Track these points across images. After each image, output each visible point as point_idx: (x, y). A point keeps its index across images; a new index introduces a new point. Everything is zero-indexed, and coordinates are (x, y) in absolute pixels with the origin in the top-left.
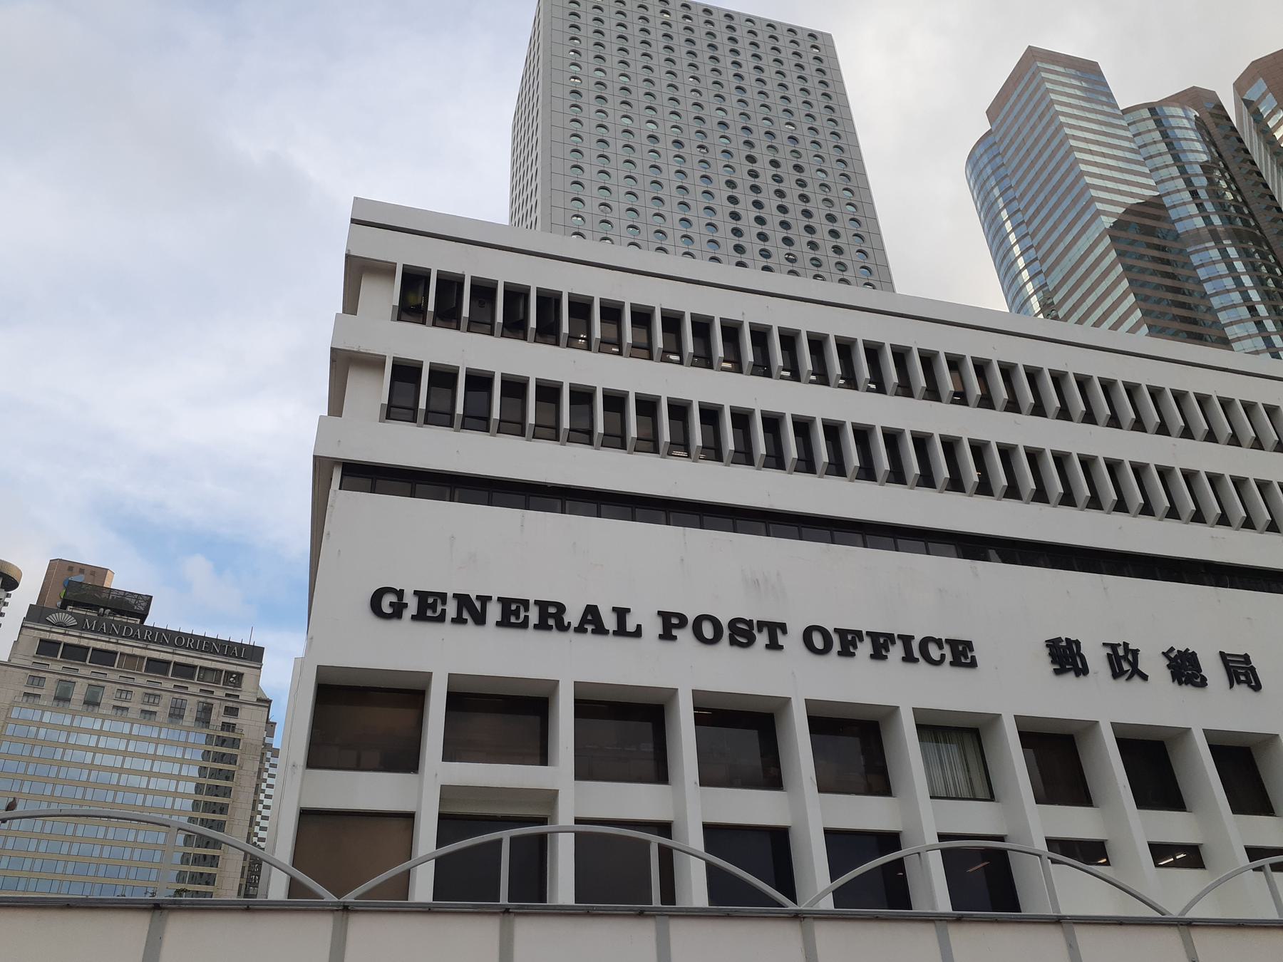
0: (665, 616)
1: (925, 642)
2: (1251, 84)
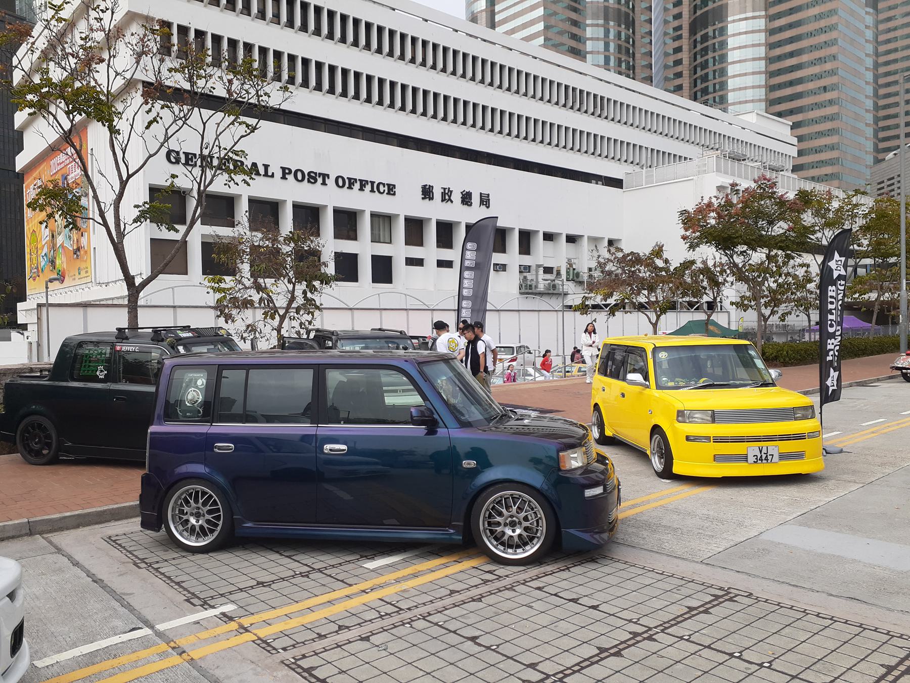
0: (283, 169)
1: (379, 184)
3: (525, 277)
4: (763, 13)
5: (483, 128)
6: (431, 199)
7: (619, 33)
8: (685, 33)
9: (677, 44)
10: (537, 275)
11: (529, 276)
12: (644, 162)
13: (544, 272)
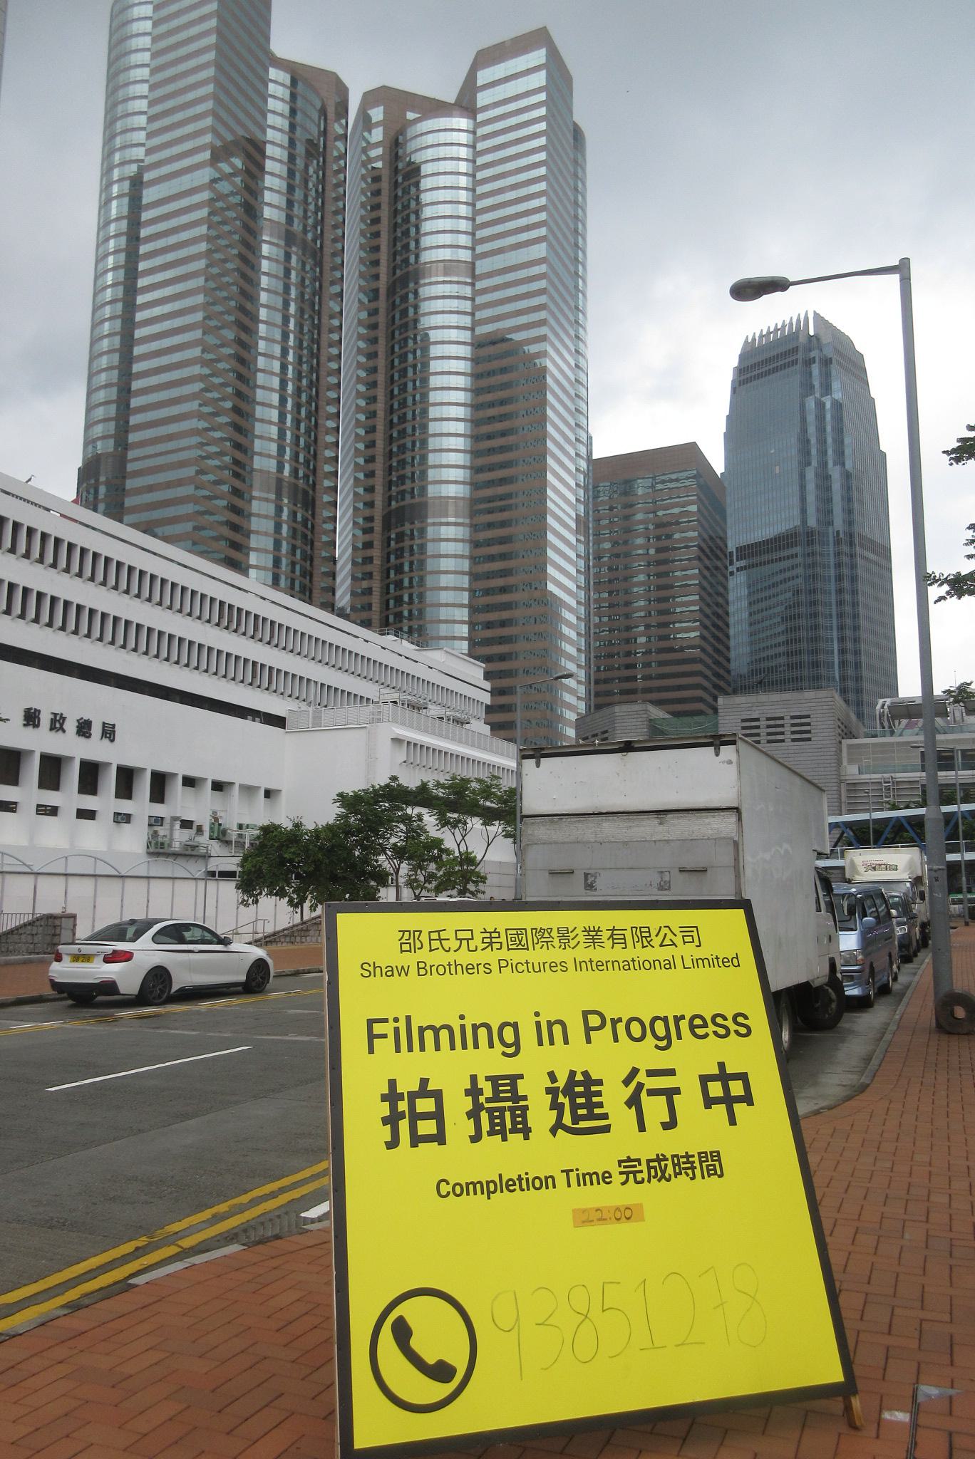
2: (375, 104)
3: (156, 832)
4: (467, 521)
5: (112, 643)
6: (36, 726)
7: (295, 514)
8: (378, 525)
9: (368, 538)
10: (172, 830)
11: (162, 831)
12: (312, 698)
13: (182, 827)
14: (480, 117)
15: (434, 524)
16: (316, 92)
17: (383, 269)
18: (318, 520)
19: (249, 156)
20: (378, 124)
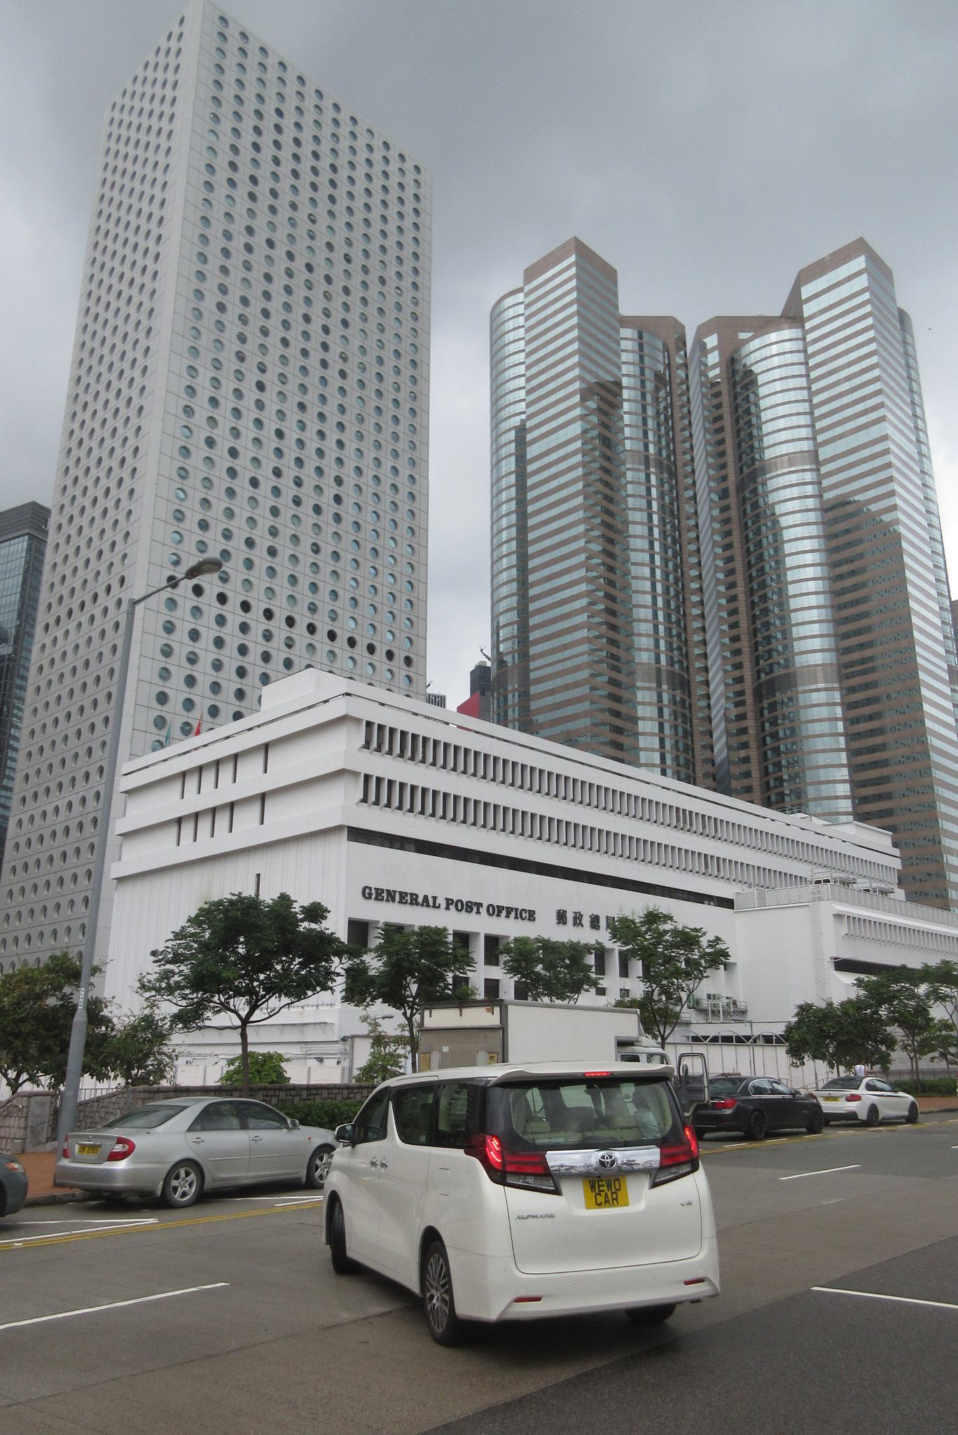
0: (447, 900)
6: (565, 923)
8: (749, 698)
9: (740, 710)
14: (808, 326)
15: (805, 692)
16: (659, 334)
17: (731, 471)
18: (694, 698)
19: (602, 399)
20: (713, 349)
